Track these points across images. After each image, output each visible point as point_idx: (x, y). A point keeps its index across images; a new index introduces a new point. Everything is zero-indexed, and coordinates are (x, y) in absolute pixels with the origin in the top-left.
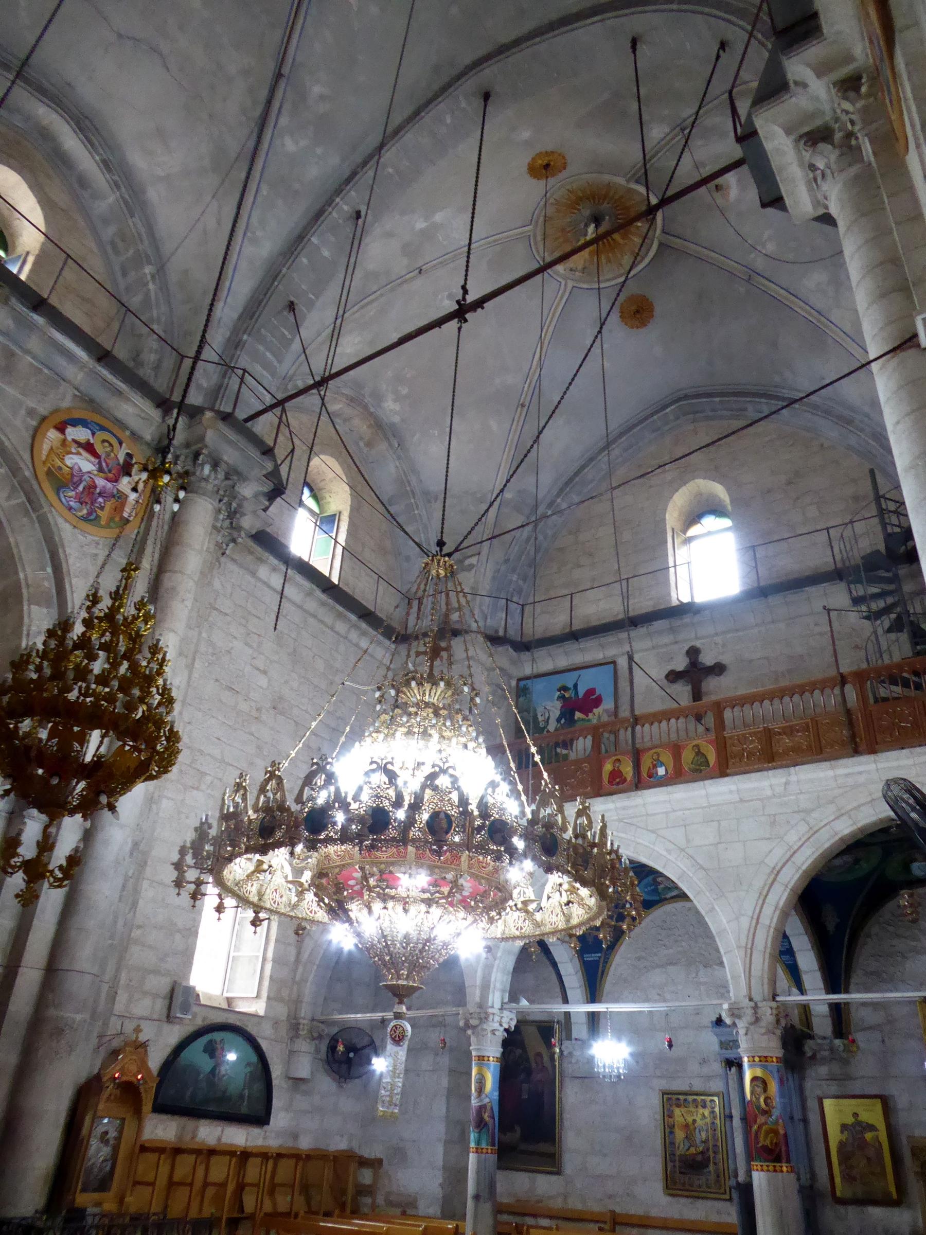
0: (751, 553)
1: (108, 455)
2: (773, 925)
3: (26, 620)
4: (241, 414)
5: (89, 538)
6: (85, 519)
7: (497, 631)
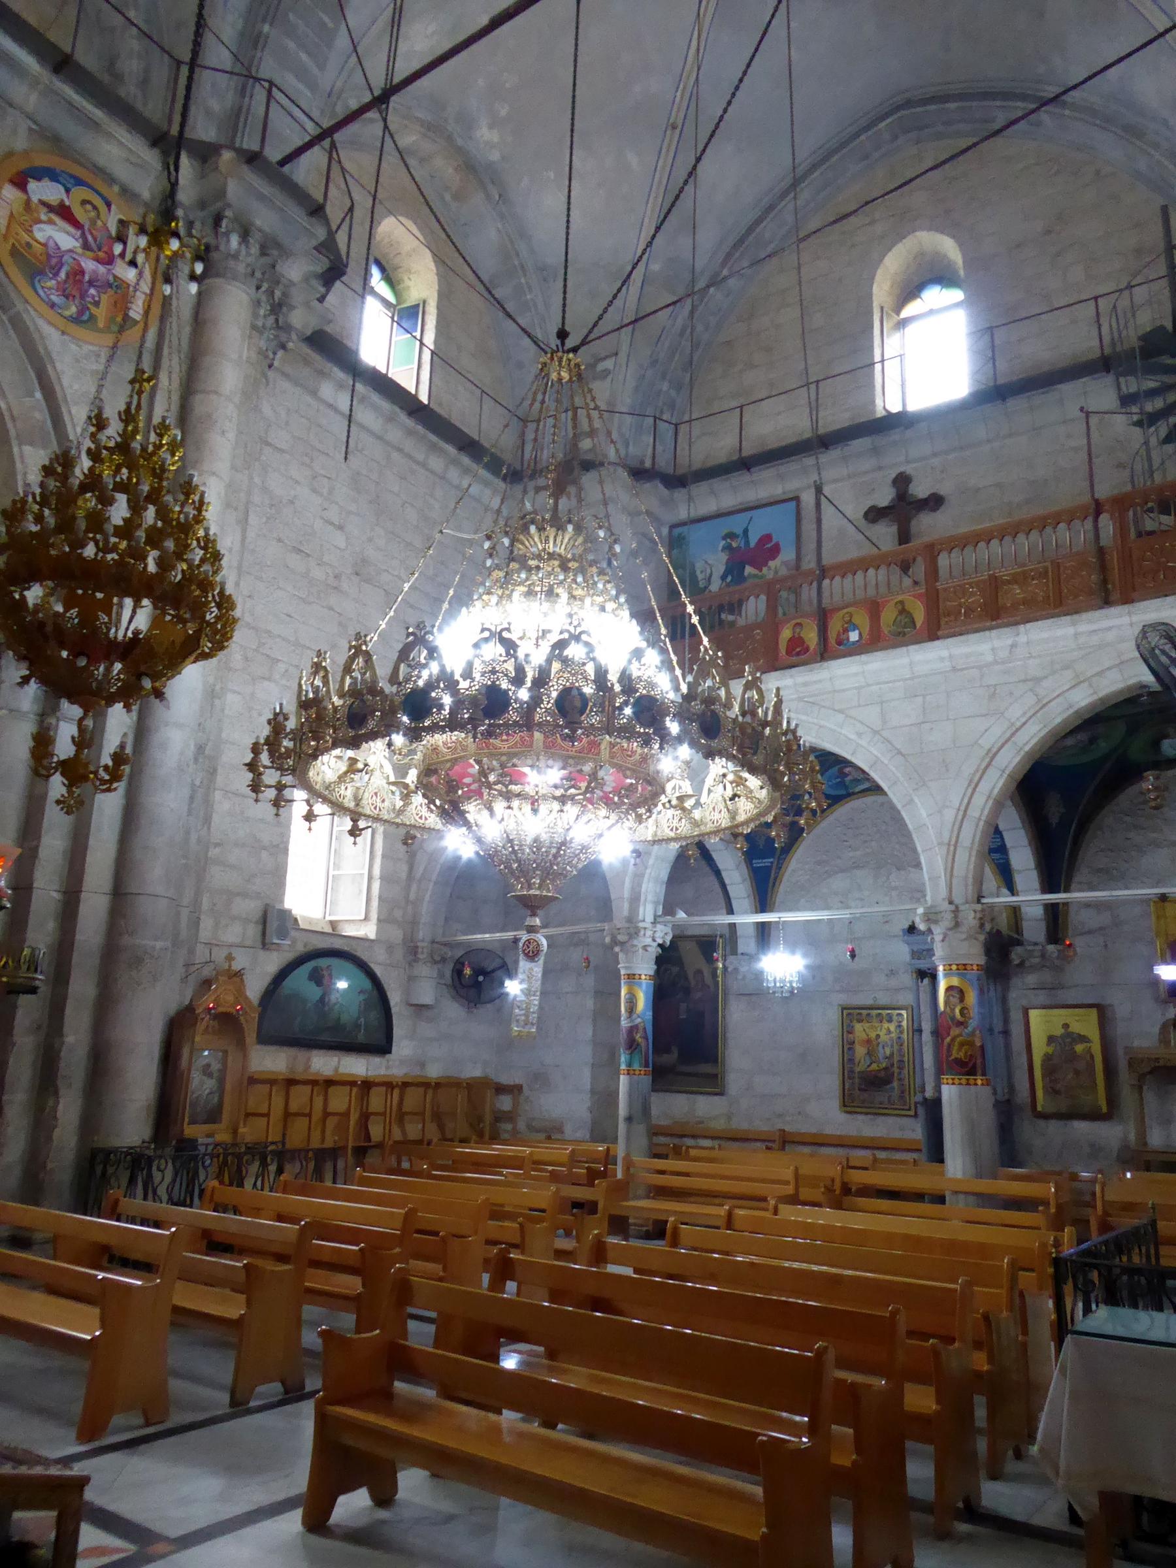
0: (987, 338)
1: (93, 222)
2: (983, 818)
3: (19, 465)
4: (274, 154)
5: (87, 348)
6: (76, 320)
7: (642, 462)
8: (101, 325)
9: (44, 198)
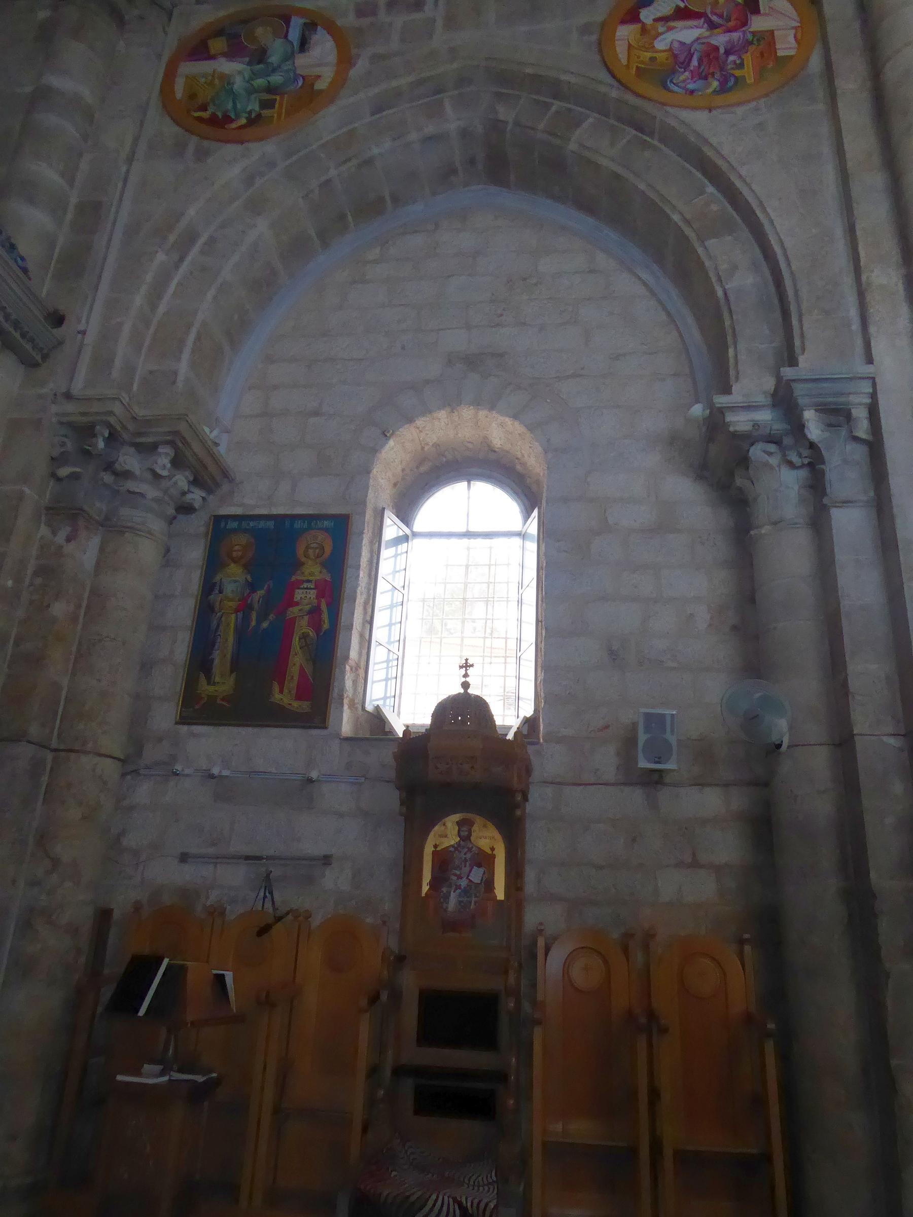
3: (707, 263)
8: (750, 80)
9: (659, 15)
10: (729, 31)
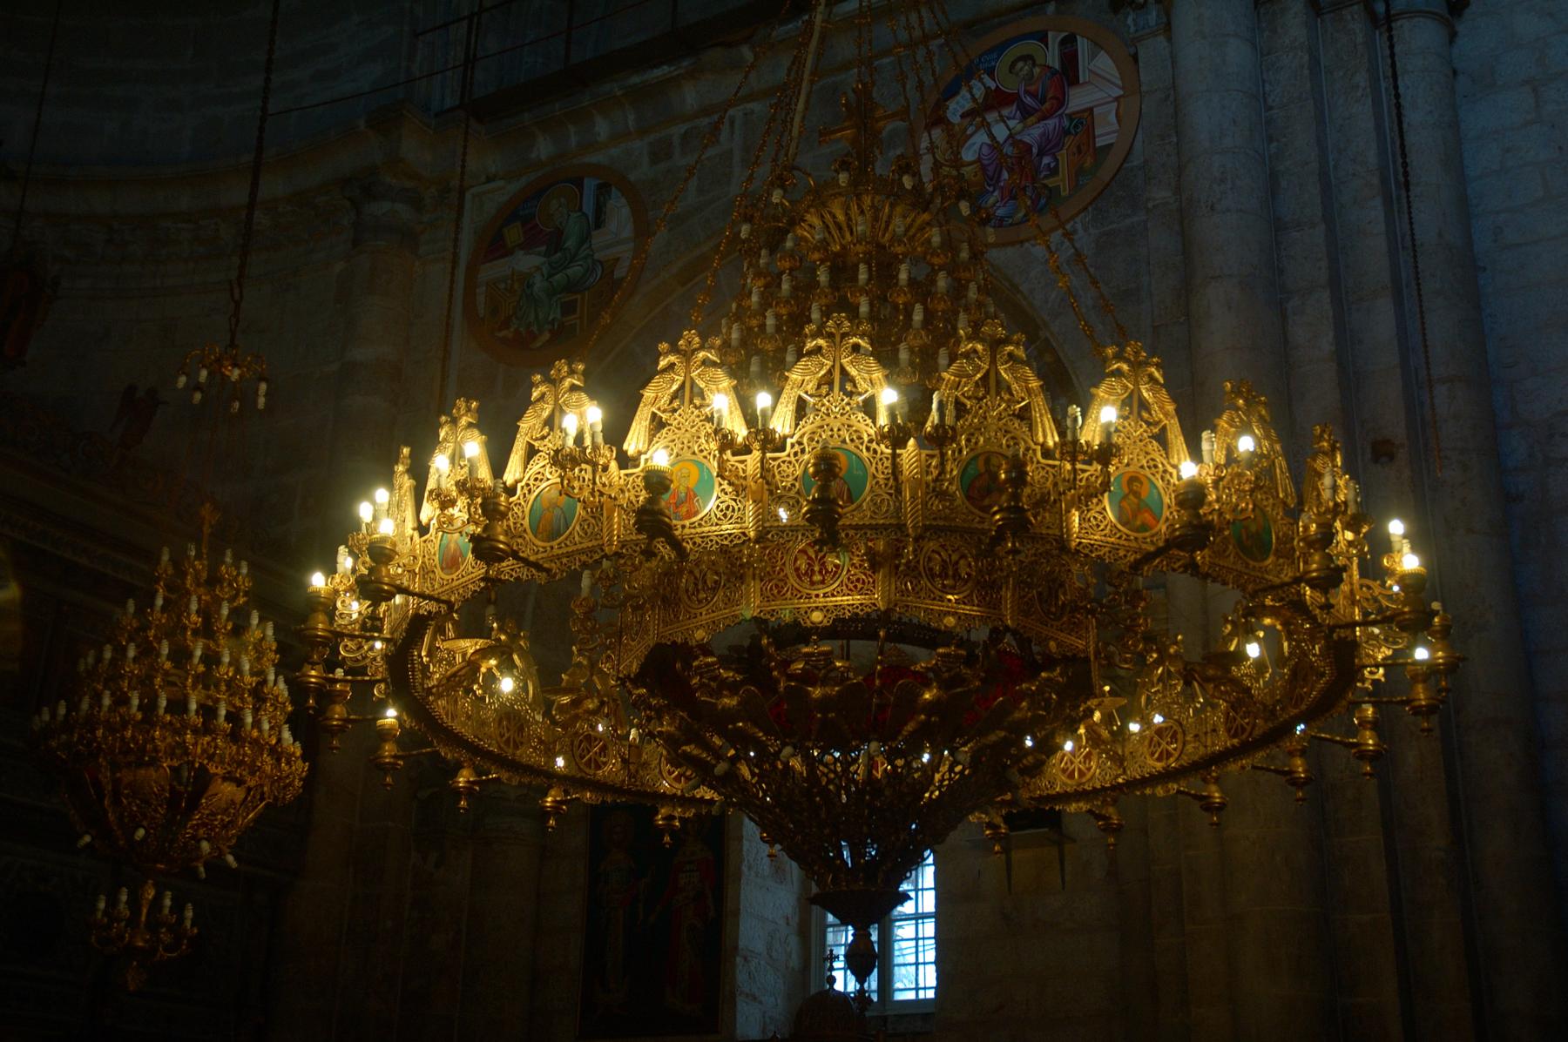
10: (1045, 118)
